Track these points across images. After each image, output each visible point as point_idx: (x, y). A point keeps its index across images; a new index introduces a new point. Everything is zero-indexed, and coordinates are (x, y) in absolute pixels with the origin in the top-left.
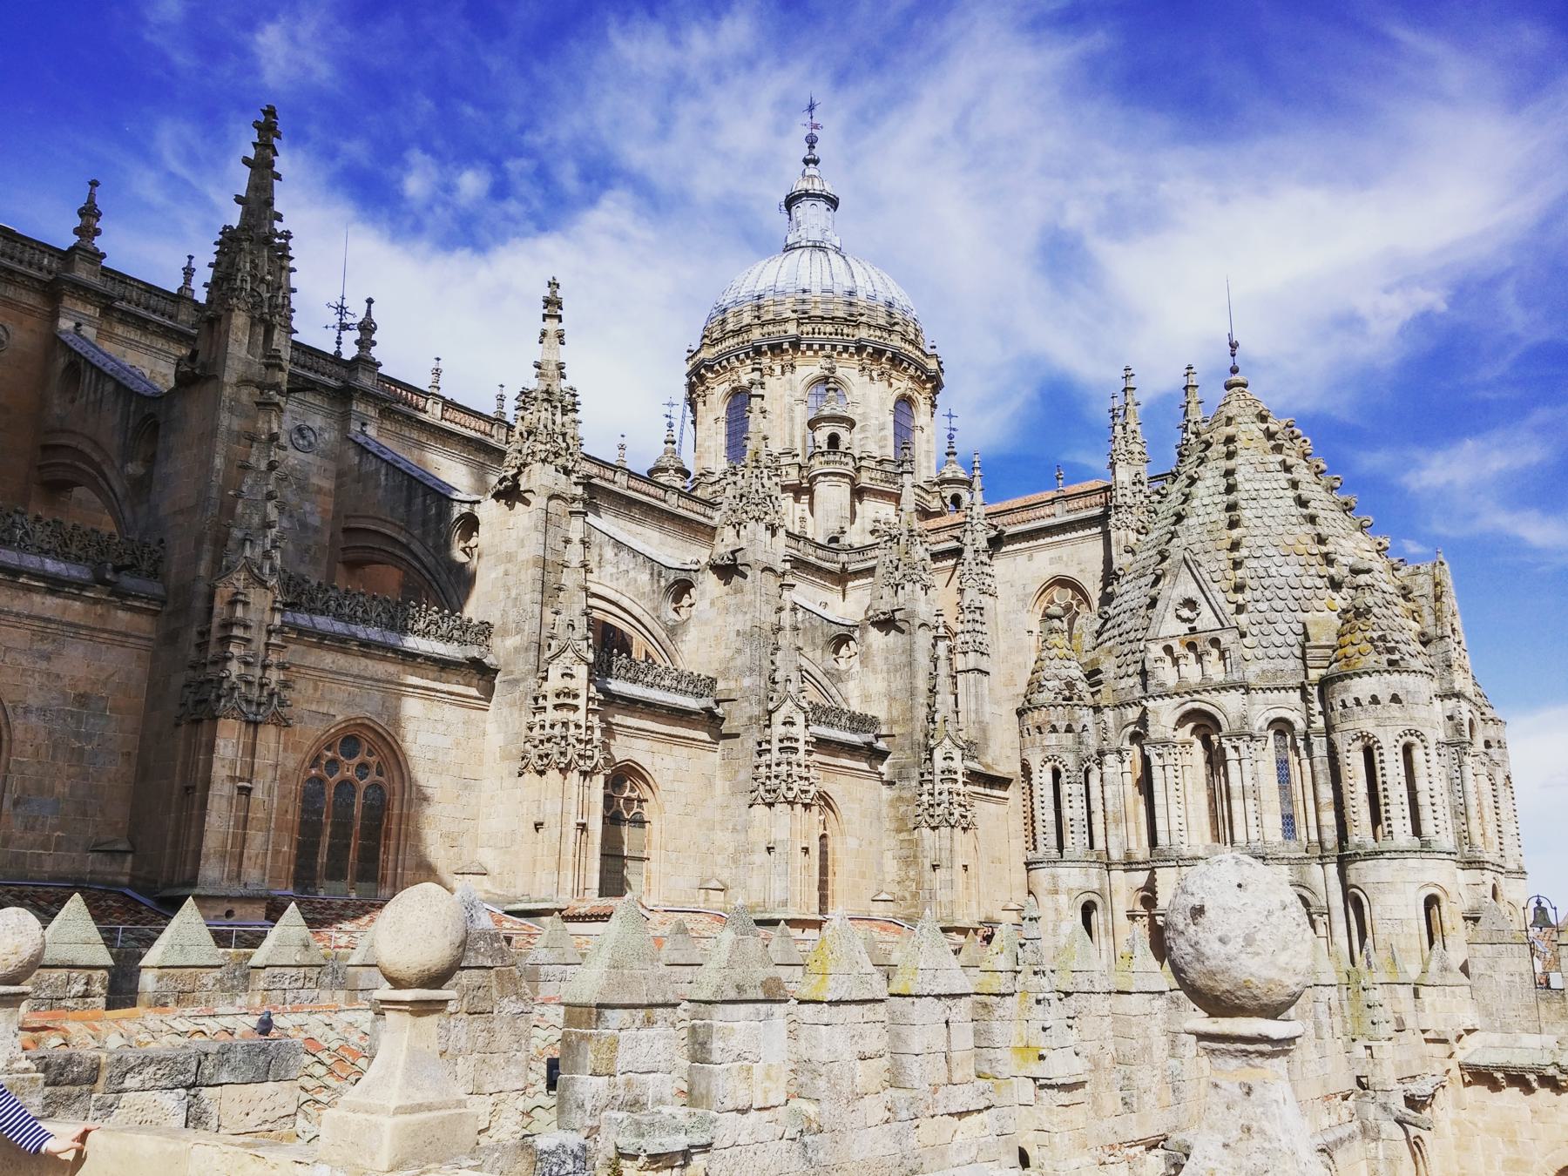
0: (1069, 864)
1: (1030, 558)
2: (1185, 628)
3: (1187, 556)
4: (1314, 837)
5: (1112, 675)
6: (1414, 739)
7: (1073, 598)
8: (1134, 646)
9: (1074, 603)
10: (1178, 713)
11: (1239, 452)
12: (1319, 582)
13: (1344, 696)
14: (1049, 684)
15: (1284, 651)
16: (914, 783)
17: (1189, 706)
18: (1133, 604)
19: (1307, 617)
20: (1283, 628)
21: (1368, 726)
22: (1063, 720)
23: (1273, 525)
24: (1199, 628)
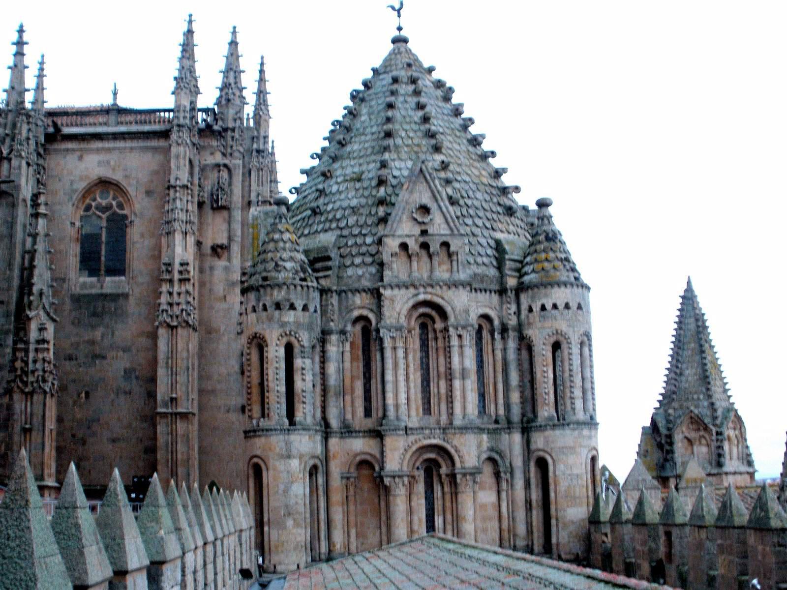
0: (301, 432)
1: (81, 158)
2: (417, 230)
3: (424, 168)
4: (501, 411)
5: (337, 263)
6: (586, 339)
7: (114, 199)
8: (359, 240)
9: (114, 203)
10: (411, 303)
11: (423, 94)
12: (500, 209)
13: (544, 301)
14: (289, 265)
15: (485, 260)
16: (9, 350)
17: (421, 297)
18: (354, 202)
19: (499, 236)
20: (483, 241)
21: (563, 326)
22: (302, 299)
23: (461, 157)
24: (430, 231)
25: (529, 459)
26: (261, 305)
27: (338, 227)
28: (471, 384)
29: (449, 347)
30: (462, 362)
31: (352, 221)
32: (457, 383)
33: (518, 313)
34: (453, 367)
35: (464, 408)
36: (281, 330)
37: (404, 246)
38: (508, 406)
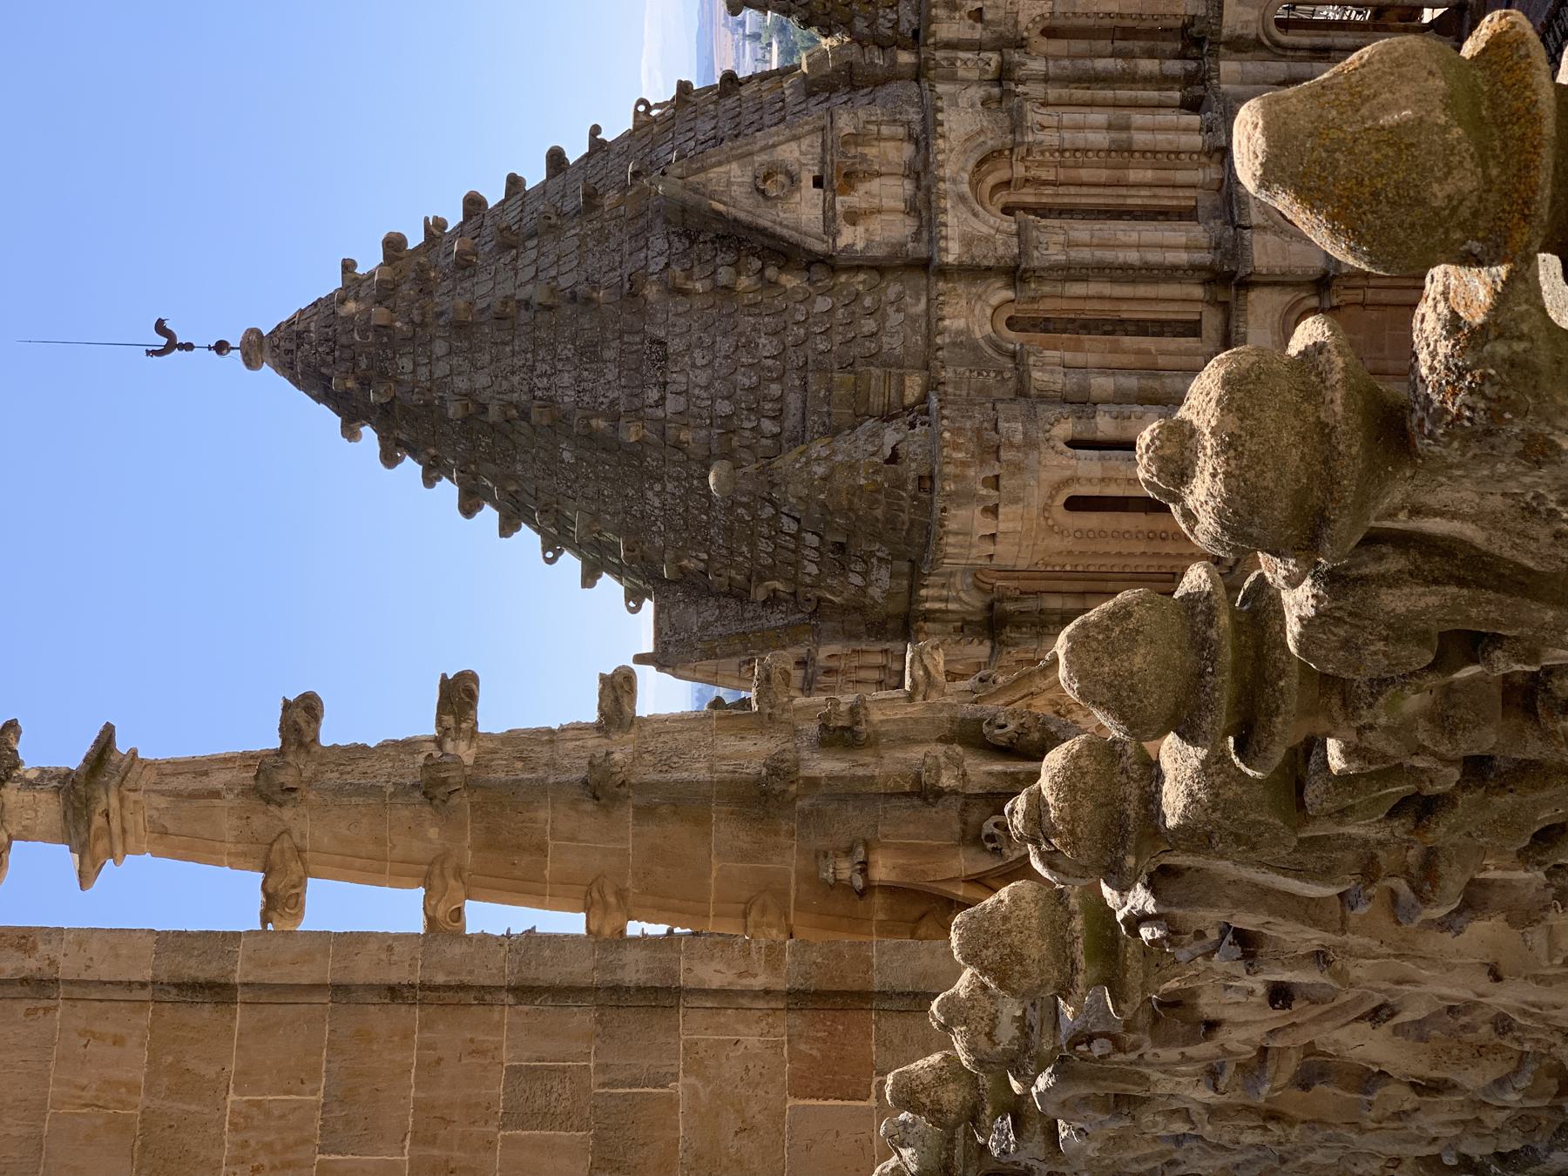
17: (965, 188)
18: (725, 345)
25: (1277, 44)
26: (984, 492)
27: (779, 379)
28: (1138, 118)
29: (1062, 151)
30: (1095, 128)
31: (767, 346)
32: (1140, 139)
33: (978, 47)
34: (1106, 145)
35: (1187, 130)
36: (1043, 447)
37: (853, 217)
38: (1163, 81)
